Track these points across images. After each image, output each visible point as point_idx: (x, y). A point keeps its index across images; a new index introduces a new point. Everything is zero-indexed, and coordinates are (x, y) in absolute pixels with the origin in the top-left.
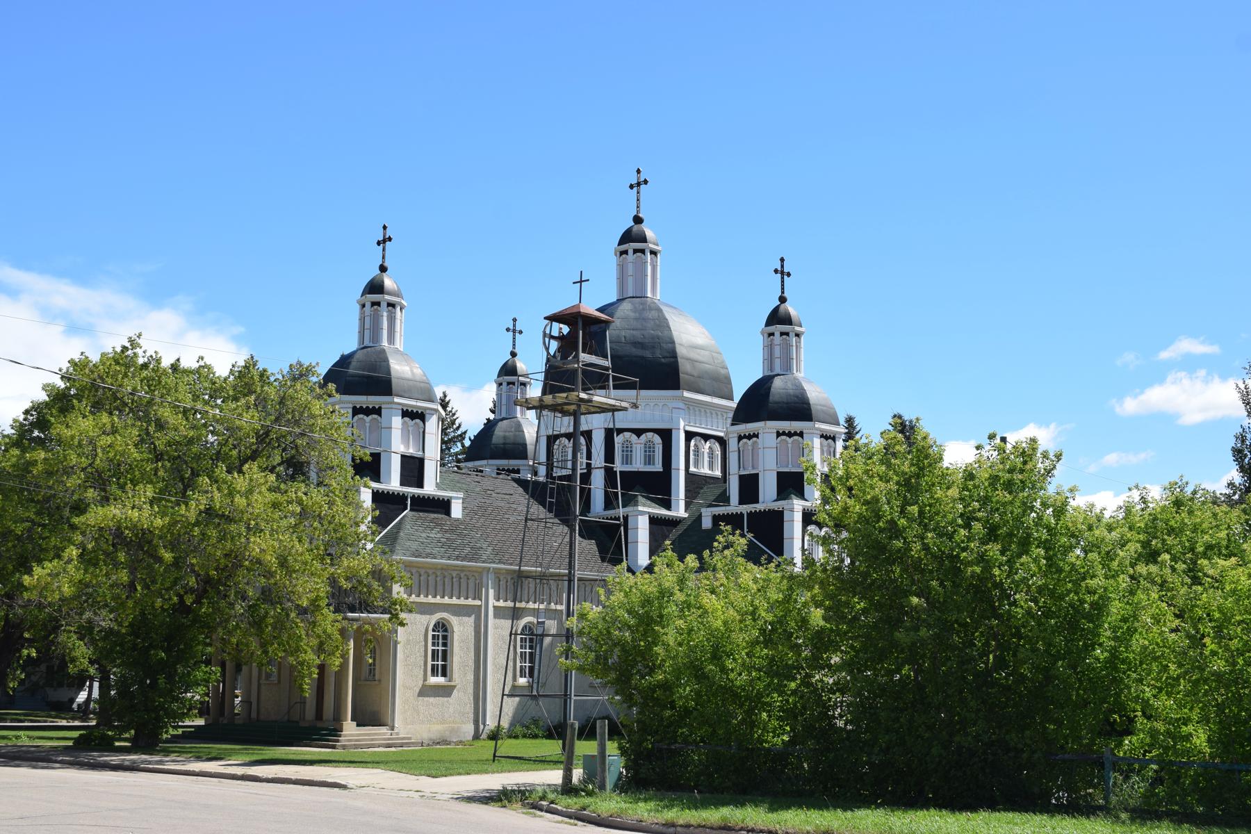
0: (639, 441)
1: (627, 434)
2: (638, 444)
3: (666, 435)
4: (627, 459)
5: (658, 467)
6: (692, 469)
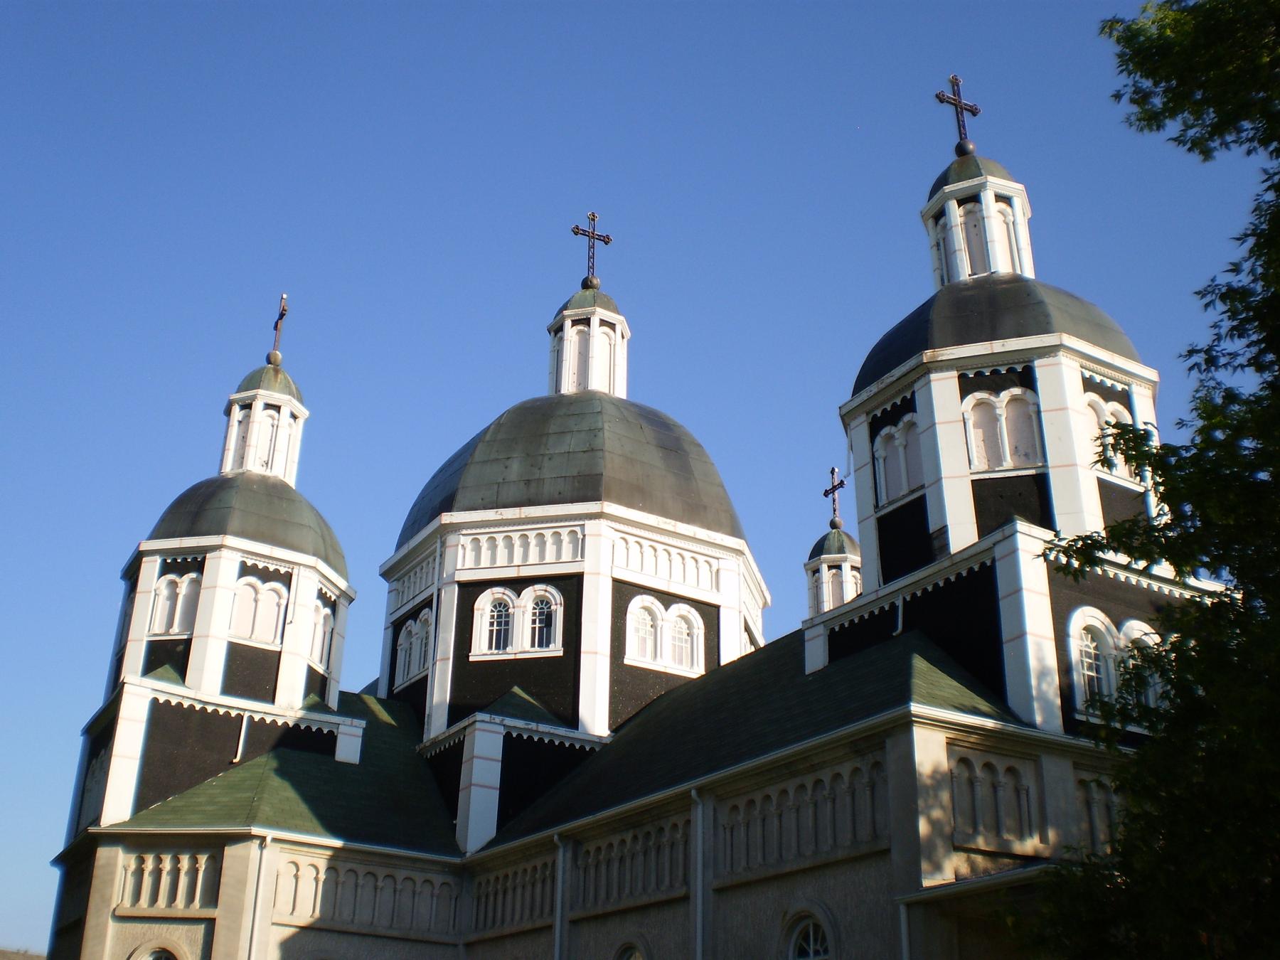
1: (498, 592)
3: (571, 586)
4: (501, 637)
5: (556, 649)
6: (633, 657)
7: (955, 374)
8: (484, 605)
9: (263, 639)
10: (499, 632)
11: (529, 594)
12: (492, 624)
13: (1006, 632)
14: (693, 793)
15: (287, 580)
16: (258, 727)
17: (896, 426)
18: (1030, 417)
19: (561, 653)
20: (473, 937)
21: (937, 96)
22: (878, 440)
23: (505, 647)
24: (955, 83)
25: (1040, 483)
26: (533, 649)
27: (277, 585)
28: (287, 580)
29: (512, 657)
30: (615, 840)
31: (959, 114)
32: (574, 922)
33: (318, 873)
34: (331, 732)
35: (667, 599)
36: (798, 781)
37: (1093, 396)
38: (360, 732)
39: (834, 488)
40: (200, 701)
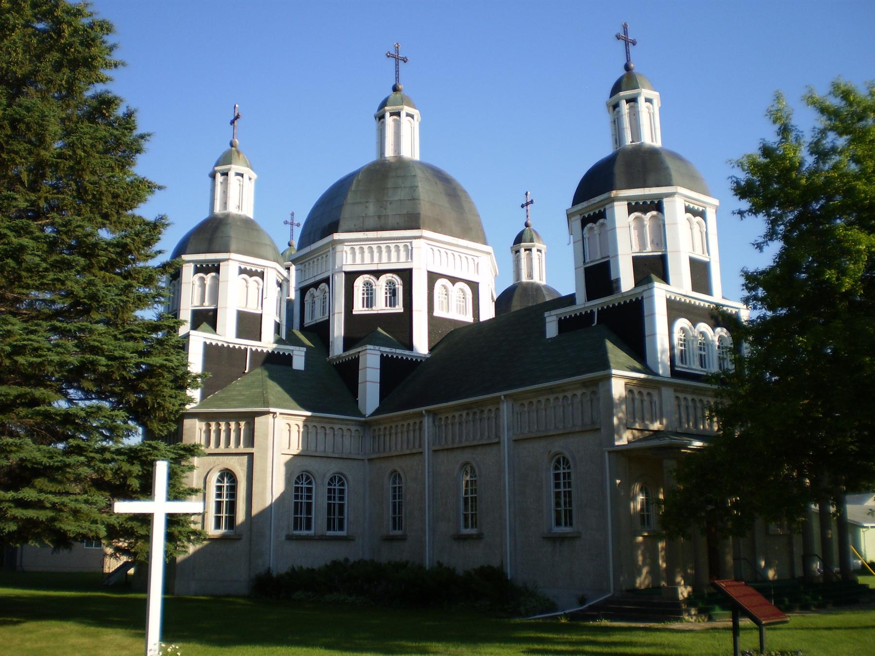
1: (366, 277)
3: (406, 275)
4: (369, 301)
5: (399, 308)
6: (437, 313)
7: (626, 203)
8: (359, 283)
9: (252, 308)
10: (367, 298)
11: (384, 278)
12: (363, 294)
13: (647, 333)
14: (502, 397)
15: (262, 275)
16: (255, 353)
17: (595, 223)
18: (660, 226)
19: (402, 311)
20: (373, 456)
21: (617, 36)
22: (586, 229)
23: (371, 307)
24: (625, 27)
25: (663, 259)
26: (386, 308)
27: (257, 278)
28: (262, 275)
29: (376, 312)
30: (457, 414)
31: (627, 45)
32: (435, 451)
33: (299, 428)
34: (289, 354)
35: (454, 280)
36: (555, 395)
37: (689, 215)
38: (303, 354)
39: (527, 204)
40: (227, 342)
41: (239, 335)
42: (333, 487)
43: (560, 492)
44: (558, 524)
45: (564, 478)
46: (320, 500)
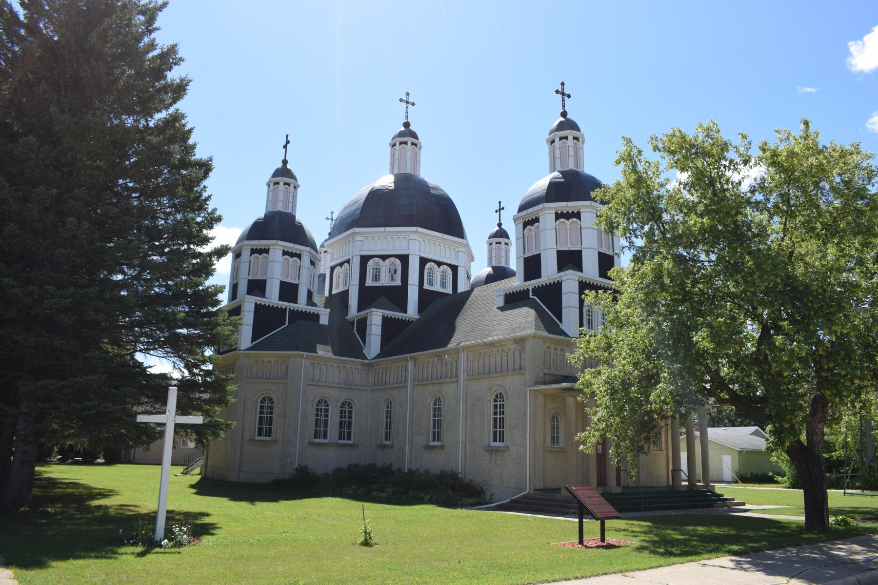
0: (384, 264)
1: (376, 259)
2: (385, 266)
3: (404, 259)
4: (376, 278)
5: (398, 282)
6: (426, 286)
8: (371, 263)
10: (376, 275)
14: (461, 349)
19: (400, 285)
20: (374, 388)
22: (526, 230)
23: (379, 281)
28: (299, 256)
29: (382, 285)
30: (431, 360)
32: (414, 386)
36: (496, 349)
38: (328, 314)
41: (280, 299)
42: (344, 409)
43: (497, 418)
44: (495, 440)
45: (500, 408)
46: (334, 418)
